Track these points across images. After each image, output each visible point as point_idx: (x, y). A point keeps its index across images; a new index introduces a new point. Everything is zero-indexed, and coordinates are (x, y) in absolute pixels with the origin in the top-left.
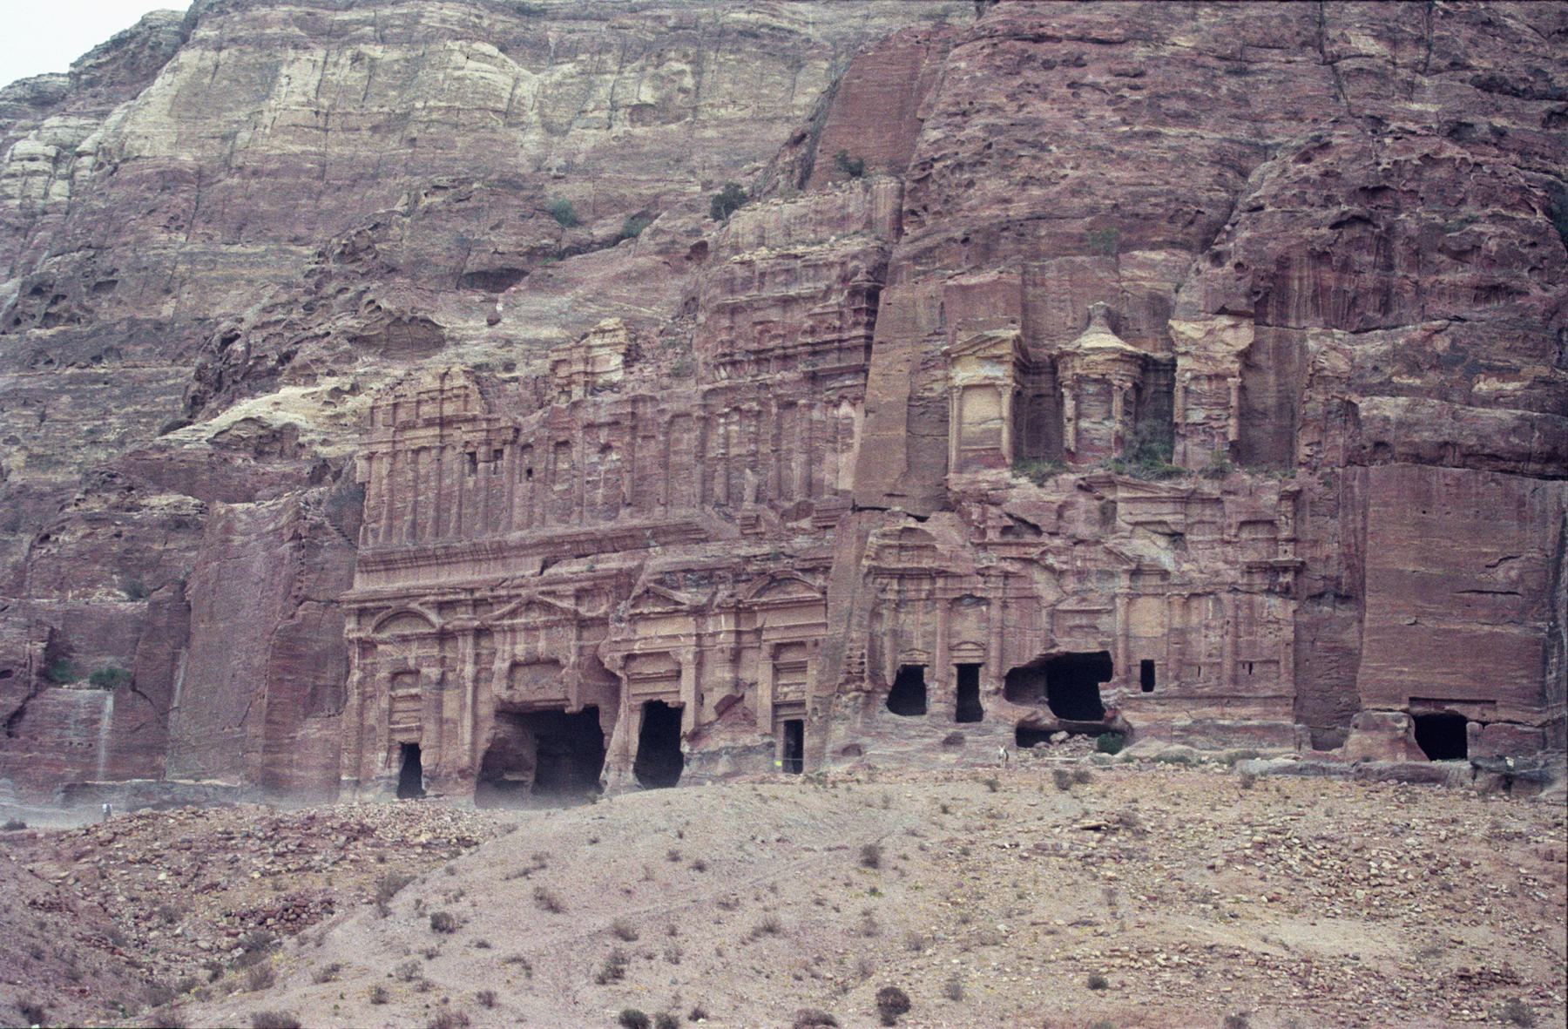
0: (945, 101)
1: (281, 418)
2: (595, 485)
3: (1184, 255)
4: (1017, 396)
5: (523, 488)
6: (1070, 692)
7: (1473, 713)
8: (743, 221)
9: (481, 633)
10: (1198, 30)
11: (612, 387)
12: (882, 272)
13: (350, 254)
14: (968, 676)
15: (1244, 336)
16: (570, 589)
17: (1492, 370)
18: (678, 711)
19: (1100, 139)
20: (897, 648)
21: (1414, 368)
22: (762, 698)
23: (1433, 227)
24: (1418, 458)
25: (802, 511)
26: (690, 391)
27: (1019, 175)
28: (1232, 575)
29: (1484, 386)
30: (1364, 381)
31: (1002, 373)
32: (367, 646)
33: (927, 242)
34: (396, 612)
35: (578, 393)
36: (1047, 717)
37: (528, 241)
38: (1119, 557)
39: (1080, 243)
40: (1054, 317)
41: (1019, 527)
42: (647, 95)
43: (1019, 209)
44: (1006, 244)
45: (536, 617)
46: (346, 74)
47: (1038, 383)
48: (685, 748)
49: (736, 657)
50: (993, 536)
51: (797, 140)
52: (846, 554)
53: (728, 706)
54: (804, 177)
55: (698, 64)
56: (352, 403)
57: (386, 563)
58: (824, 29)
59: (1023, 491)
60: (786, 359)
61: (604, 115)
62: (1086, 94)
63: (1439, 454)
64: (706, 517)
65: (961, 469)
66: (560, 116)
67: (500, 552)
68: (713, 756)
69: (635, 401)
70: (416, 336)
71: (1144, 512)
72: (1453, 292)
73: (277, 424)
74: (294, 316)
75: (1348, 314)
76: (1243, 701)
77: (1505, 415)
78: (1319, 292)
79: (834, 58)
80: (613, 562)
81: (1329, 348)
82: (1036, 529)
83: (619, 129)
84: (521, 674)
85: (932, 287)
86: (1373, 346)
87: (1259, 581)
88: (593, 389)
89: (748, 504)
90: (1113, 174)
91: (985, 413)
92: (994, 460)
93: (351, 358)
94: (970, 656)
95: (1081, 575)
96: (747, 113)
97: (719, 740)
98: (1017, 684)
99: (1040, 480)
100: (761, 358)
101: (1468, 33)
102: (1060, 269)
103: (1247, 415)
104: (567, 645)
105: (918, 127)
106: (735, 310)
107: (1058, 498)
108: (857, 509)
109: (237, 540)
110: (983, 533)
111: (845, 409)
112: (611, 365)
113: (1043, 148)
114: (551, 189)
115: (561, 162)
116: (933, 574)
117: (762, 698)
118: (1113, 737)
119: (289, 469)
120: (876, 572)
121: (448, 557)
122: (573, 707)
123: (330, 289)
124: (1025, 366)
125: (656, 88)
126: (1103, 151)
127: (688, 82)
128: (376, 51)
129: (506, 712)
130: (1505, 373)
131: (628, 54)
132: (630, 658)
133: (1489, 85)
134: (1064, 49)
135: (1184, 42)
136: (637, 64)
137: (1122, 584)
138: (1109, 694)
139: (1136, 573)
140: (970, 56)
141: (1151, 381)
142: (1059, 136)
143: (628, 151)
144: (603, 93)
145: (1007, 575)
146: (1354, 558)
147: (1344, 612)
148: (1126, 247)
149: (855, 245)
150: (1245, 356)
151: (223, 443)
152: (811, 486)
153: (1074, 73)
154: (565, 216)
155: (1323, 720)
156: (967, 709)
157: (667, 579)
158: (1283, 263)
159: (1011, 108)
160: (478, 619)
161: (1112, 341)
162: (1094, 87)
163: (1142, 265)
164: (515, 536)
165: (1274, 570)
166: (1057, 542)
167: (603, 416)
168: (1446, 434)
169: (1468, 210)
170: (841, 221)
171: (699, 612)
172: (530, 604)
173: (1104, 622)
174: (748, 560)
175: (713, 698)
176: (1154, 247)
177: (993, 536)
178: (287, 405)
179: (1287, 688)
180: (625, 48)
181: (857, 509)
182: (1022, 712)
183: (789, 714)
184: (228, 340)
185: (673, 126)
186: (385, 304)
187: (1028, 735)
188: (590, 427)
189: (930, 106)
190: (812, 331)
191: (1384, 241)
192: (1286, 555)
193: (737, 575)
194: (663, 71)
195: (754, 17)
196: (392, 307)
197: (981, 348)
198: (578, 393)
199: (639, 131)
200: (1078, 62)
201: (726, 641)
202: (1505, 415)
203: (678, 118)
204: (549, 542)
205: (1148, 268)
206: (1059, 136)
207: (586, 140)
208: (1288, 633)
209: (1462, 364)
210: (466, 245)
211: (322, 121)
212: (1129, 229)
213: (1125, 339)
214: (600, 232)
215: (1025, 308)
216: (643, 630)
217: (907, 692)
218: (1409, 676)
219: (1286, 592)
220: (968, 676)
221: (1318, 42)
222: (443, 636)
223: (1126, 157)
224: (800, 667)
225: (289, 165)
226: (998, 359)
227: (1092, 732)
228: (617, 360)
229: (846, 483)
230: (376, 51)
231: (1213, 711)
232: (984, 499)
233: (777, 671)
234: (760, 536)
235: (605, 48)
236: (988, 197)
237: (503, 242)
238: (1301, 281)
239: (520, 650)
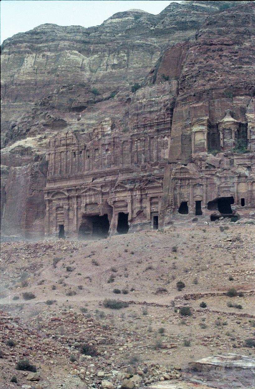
0: (188, 61)
1: (28, 145)
2: (105, 159)
3: (249, 97)
4: (208, 134)
5: (87, 161)
6: (224, 207)
8: (139, 93)
9: (78, 197)
10: (251, 41)
11: (108, 135)
13: (43, 104)
14: (198, 204)
16: (100, 185)
19: (227, 69)
20: (181, 197)
22: (148, 211)
25: (156, 164)
26: (128, 135)
27: (207, 79)
31: (204, 128)
32: (50, 201)
33: (185, 96)
35: (100, 137)
36: (218, 213)
37: (87, 100)
38: (235, 173)
39: (223, 95)
40: (218, 114)
41: (210, 166)
42: (116, 62)
43: (208, 87)
44: (205, 96)
45: (91, 193)
46: (41, 59)
48: (129, 224)
49: (141, 201)
50: (203, 169)
51: (152, 72)
53: (139, 213)
54: (154, 81)
56: (44, 141)
57: (54, 180)
58: (159, 44)
59: (211, 158)
60: (151, 127)
61: (105, 67)
62: (223, 58)
64: (133, 166)
65: (195, 152)
66: (94, 68)
67: (82, 177)
68: (136, 226)
69: (114, 138)
70: (59, 124)
73: (26, 147)
74: (30, 120)
79: (162, 51)
80: (110, 178)
82: (214, 167)
83: (109, 71)
84: (88, 207)
85: (186, 107)
88: (104, 135)
89: (143, 163)
90: (230, 78)
91: (201, 138)
92: (203, 150)
93: (44, 130)
95: (226, 178)
96: (140, 66)
97: (137, 222)
98: (210, 205)
99: (215, 155)
100: (145, 126)
102: (218, 102)
104: (99, 199)
105: (182, 67)
106: (138, 115)
107: (219, 159)
109: (17, 176)
110: (201, 168)
111: (166, 138)
112: (108, 129)
113: (213, 72)
114: (92, 86)
115: (95, 79)
116: (189, 179)
117: (148, 211)
118: (235, 218)
119: (30, 158)
120: (175, 179)
121: (69, 179)
122: (101, 215)
123: (39, 112)
124: (210, 126)
125: (118, 60)
126: (228, 72)
127: (126, 58)
129: (85, 216)
131: (110, 52)
132: (115, 202)
135: (247, 44)
136: (113, 54)
137: (236, 179)
138: (233, 207)
139: (239, 177)
140: (194, 50)
141: (241, 129)
142: (217, 69)
143: (111, 76)
144: (105, 62)
145: (207, 178)
148: (234, 96)
149: (167, 97)
151: (13, 152)
152: (158, 158)
153: (220, 53)
154: (95, 93)
156: (198, 212)
159: (205, 62)
160: (76, 193)
161: (231, 119)
162: (225, 56)
163: (238, 100)
164: (86, 173)
166: (219, 170)
167: (106, 142)
170: (164, 92)
171: (131, 190)
172: (90, 190)
173: (231, 189)
174: (143, 177)
175: (136, 211)
176: (242, 95)
177: (203, 169)
178: (29, 142)
180: (110, 51)
182: (212, 212)
183: (155, 215)
184: (13, 126)
185: (122, 69)
186: (52, 116)
187: (214, 218)
188: (103, 145)
189: (185, 62)
190: (157, 119)
193: (141, 181)
194: (119, 56)
195: (141, 41)
196: (54, 117)
197: (199, 122)
198: (100, 137)
199: (114, 71)
200: (221, 50)
201: (138, 197)
203: (123, 67)
204: (94, 174)
205: (240, 101)
207: (101, 73)
210: (71, 100)
211: (35, 71)
212: (235, 91)
213: (235, 119)
214: (104, 97)
215: (210, 112)
216: (118, 195)
217: (183, 208)
220: (198, 204)
222: (69, 198)
223: (233, 73)
224: (157, 203)
225: (28, 82)
226: (203, 125)
227: (230, 217)
228: (109, 128)
229: (167, 157)
230: (48, 54)
232: (201, 160)
233: (151, 204)
234: (146, 171)
235: (105, 51)
236: (200, 85)
237: (81, 100)
239: (88, 201)
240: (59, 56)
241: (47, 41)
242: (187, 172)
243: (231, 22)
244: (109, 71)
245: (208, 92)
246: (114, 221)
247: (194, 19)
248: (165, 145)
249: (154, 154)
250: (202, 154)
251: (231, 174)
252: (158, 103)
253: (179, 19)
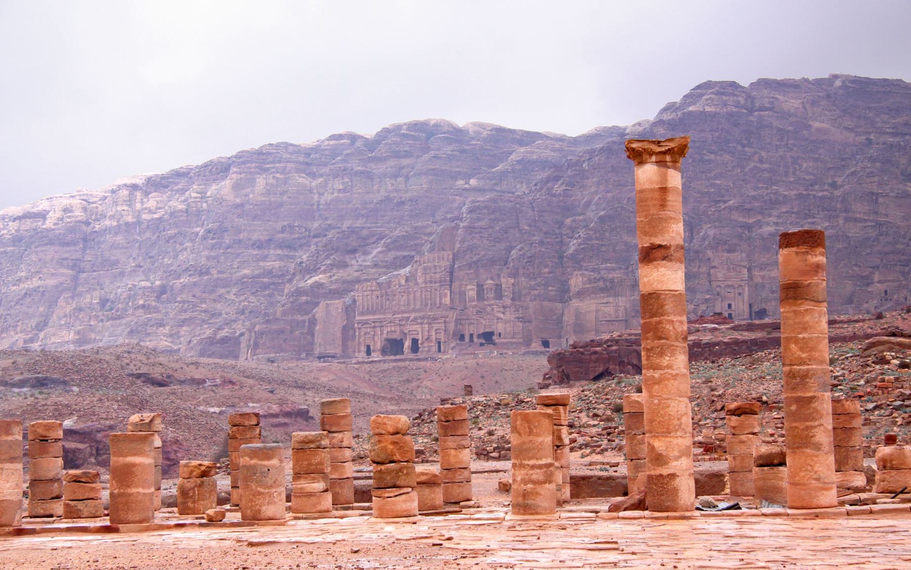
14: (471, 335)
15: (512, 281)
22: (434, 337)
29: (550, 288)
31: (475, 287)
36: (483, 341)
78: (524, 273)
92: (473, 301)
94: (471, 332)
98: (479, 336)
100: (431, 282)
103: (514, 293)
117: (434, 337)
134: (478, 230)
150: (513, 284)
152: (440, 303)
156: (471, 340)
193: (428, 318)
202: (553, 293)
220: (471, 335)
238: (521, 271)
243: (485, 211)
247: (407, 148)
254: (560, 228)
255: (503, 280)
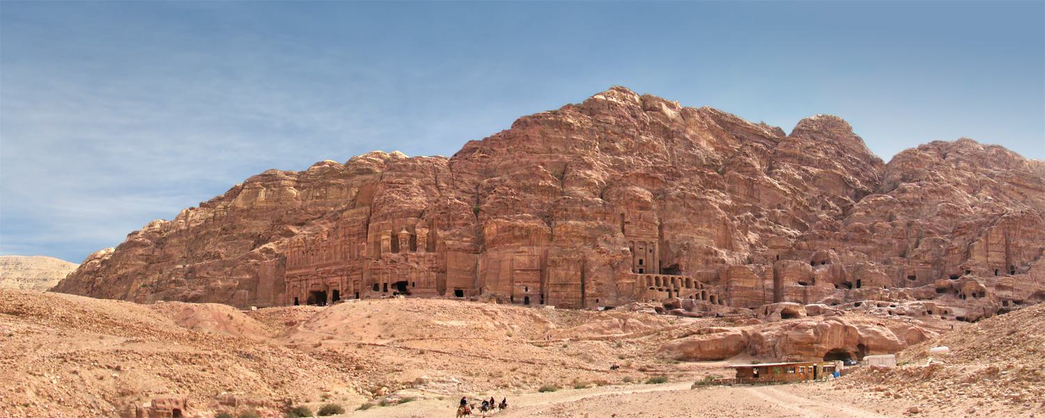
0: (377, 193)
1: (270, 247)
4: (392, 241)
5: (312, 257)
7: (464, 290)
8: (345, 214)
9: (306, 280)
11: (326, 241)
12: (368, 222)
13: (278, 221)
14: (385, 285)
15: (427, 231)
17: (465, 237)
18: (338, 291)
21: (454, 237)
22: (352, 288)
23: (456, 214)
24: (455, 250)
25: (357, 259)
28: (426, 269)
29: (465, 239)
30: (446, 238)
31: (389, 237)
32: (288, 282)
34: (293, 277)
35: (320, 242)
38: (409, 266)
39: (401, 216)
40: (397, 228)
41: (392, 262)
42: (318, 195)
43: (390, 211)
44: (389, 217)
45: (315, 277)
47: (395, 239)
49: (347, 283)
50: (389, 263)
51: (353, 201)
52: (365, 266)
53: (346, 290)
55: (326, 189)
56: (281, 245)
57: (291, 269)
60: (353, 236)
63: (458, 250)
66: (304, 198)
67: (309, 267)
71: (412, 259)
72: (459, 225)
75: (442, 228)
76: (428, 288)
77: (468, 244)
80: (327, 268)
81: (440, 233)
83: (314, 200)
84: (314, 286)
85: (377, 223)
86: (447, 233)
87: (431, 270)
88: (323, 241)
91: (386, 242)
92: (389, 251)
94: (386, 282)
95: (403, 269)
97: (345, 296)
100: (349, 235)
101: (459, 183)
103: (427, 243)
104: (320, 281)
105: (373, 198)
106: (345, 228)
108: (367, 259)
111: (363, 243)
112: (325, 237)
120: (370, 269)
121: (301, 268)
122: (322, 291)
124: (393, 236)
128: (274, 189)
129: (311, 292)
130: (468, 237)
131: (314, 188)
132: (331, 283)
133: (463, 191)
137: (409, 270)
138: (407, 287)
139: (411, 269)
144: (311, 195)
146: (445, 267)
147: (443, 274)
148: (408, 217)
149: (363, 217)
150: (427, 234)
152: (358, 255)
155: (442, 292)
156: (386, 290)
157: (336, 271)
158: (433, 219)
160: (306, 277)
161: (406, 232)
164: (311, 265)
165: (433, 268)
168: (460, 246)
169: (461, 211)
170: (361, 213)
171: (341, 276)
175: (344, 289)
177: (389, 263)
178: (270, 245)
179: (435, 286)
181: (367, 259)
182: (395, 290)
184: (259, 235)
188: (323, 247)
191: (449, 216)
192: (435, 265)
197: (386, 233)
198: (320, 242)
201: (346, 280)
202: (468, 244)
204: (317, 265)
205: (411, 220)
206: (396, 200)
208: (435, 278)
209: (461, 236)
211: (267, 201)
215: (393, 227)
216: (332, 279)
217: (376, 288)
218: (455, 284)
219: (435, 271)
220: (385, 285)
221: (436, 184)
222: (301, 280)
224: (358, 284)
229: (364, 255)
230: (274, 189)
231: (423, 290)
233: (354, 285)
239: (313, 282)
240: (281, 190)
241: (272, 180)
242: (378, 265)
244: (314, 200)
245: (391, 214)
246: (330, 295)
248: (363, 248)
249: (356, 253)
250: (387, 254)
251: (406, 267)
252: (358, 221)
253: (358, 166)
254: (477, 188)
255: (418, 230)
